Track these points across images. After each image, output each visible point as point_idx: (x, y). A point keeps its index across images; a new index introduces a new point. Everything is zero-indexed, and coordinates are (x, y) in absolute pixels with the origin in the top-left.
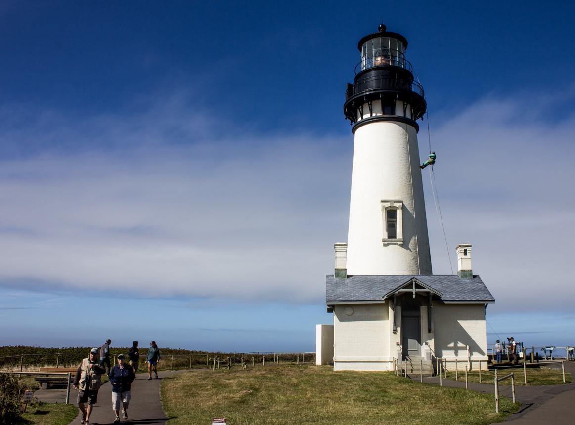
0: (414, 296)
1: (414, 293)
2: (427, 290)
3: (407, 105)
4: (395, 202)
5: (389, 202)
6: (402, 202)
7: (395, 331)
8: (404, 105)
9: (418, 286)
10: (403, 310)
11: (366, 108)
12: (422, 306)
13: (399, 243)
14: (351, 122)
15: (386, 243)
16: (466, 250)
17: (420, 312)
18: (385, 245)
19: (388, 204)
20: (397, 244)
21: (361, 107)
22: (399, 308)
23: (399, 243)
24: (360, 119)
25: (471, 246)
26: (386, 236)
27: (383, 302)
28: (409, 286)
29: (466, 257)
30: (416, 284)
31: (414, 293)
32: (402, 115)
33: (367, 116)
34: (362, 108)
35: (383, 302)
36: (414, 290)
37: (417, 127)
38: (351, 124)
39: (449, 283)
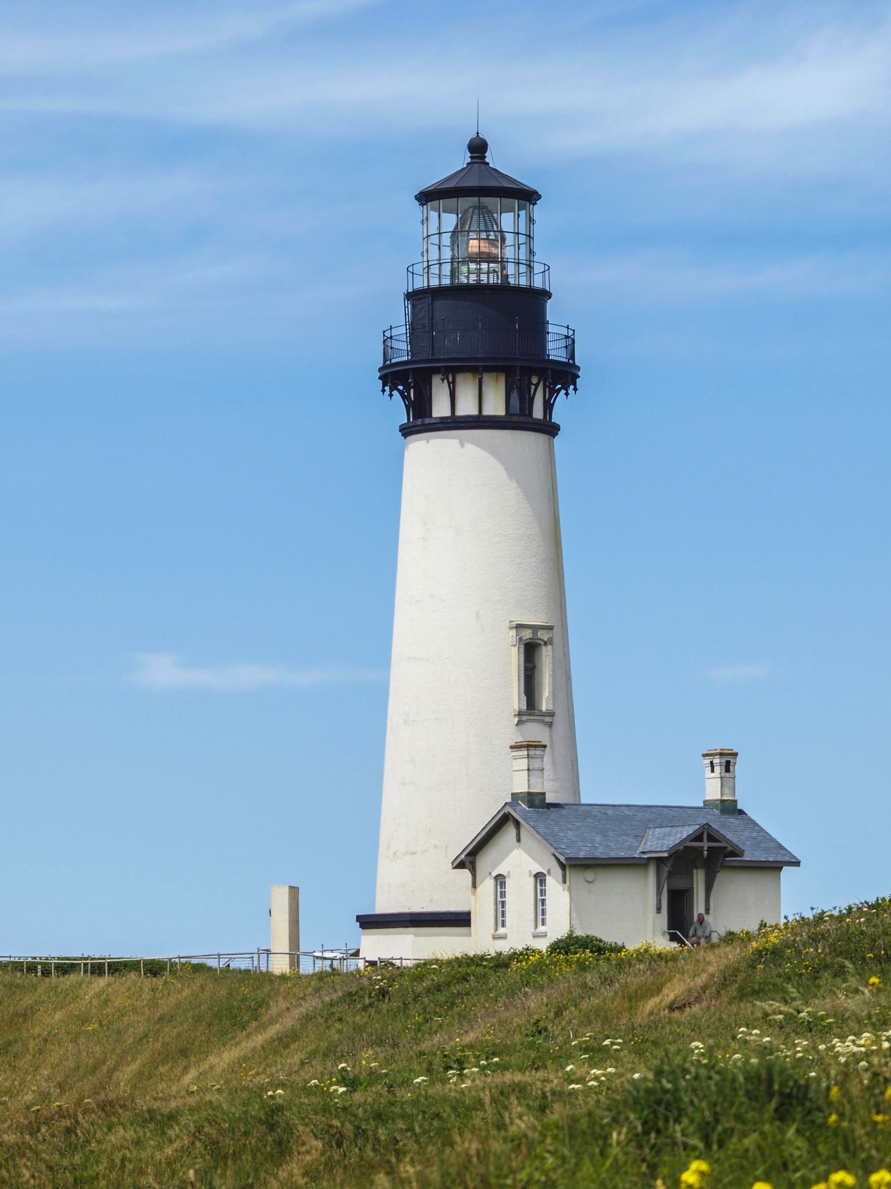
1: (706, 848)
7: (659, 910)
9: (711, 838)
12: (697, 868)
14: (384, 386)
15: (524, 718)
17: (692, 878)
20: (542, 721)
23: (548, 719)
24: (440, 408)
28: (698, 837)
29: (727, 775)
33: (467, 407)
34: (454, 382)
37: (550, 429)
38: (383, 391)
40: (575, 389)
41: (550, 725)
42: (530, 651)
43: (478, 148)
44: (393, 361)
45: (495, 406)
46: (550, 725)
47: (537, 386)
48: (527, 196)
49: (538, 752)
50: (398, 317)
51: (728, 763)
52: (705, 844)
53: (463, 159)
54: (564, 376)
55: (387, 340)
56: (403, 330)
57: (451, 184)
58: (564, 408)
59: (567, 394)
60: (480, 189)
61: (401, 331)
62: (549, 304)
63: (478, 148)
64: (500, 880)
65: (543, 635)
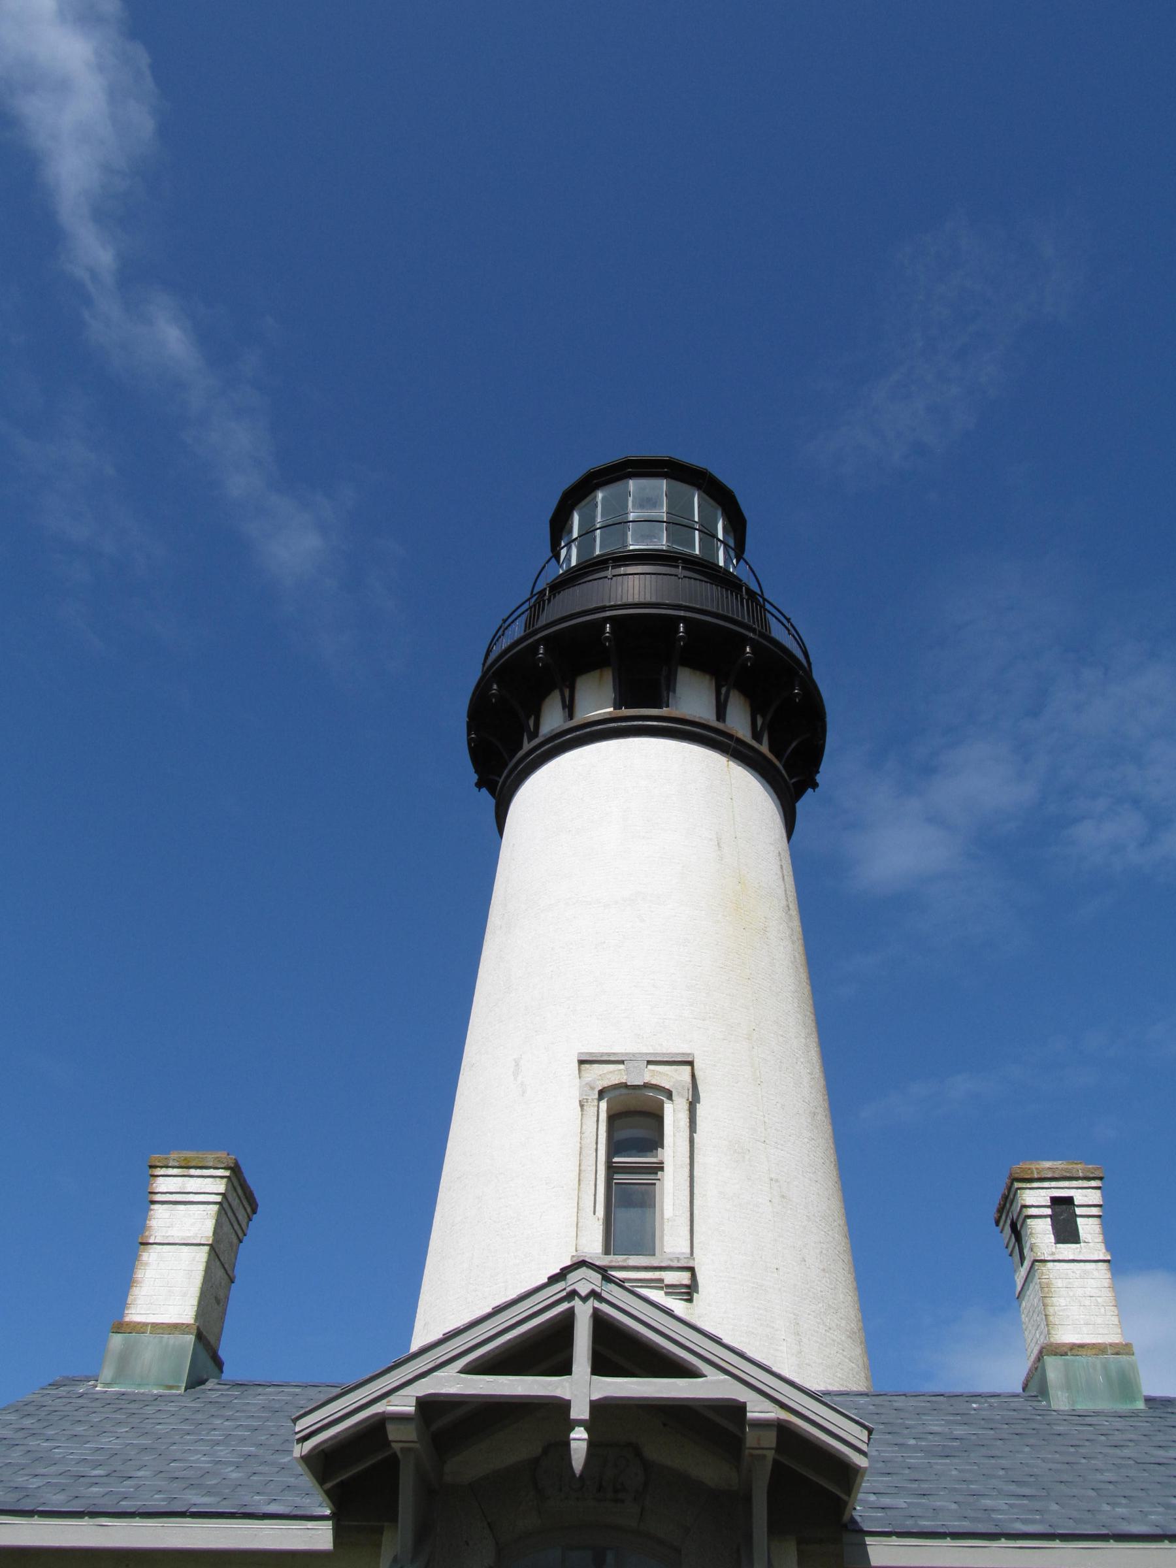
0: (579, 1434)
1: (580, 1411)
2: (710, 1387)
4: (649, 1062)
5: (622, 1062)
6: (691, 1063)
9: (620, 1349)
13: (671, 1277)
16: (1069, 1201)
23: (671, 1277)
29: (1067, 1250)
30: (600, 1323)
31: (580, 1411)
51: (1063, 1209)
52: (580, 1388)
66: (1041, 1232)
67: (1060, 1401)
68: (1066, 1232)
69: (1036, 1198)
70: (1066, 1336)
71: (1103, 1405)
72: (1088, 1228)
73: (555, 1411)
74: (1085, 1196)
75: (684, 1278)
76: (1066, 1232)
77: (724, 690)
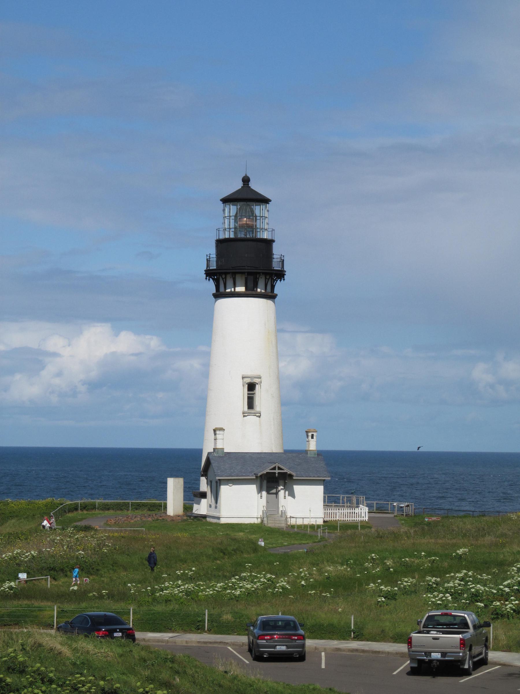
3: (268, 279)
8: (266, 278)
9: (279, 468)
10: (268, 482)
11: (230, 282)
13: (257, 415)
15: (246, 414)
18: (244, 416)
19: (248, 380)
20: (255, 415)
21: (224, 276)
22: (265, 483)
23: (257, 415)
24: (222, 289)
25: (316, 432)
26: (246, 408)
27: (254, 477)
28: (274, 468)
29: (312, 440)
32: (263, 291)
34: (226, 278)
35: (254, 477)
36: (277, 471)
38: (209, 280)
39: (300, 461)
40: (284, 280)
41: (259, 417)
42: (251, 387)
43: (246, 180)
44: (211, 268)
45: (241, 289)
46: (259, 417)
47: (258, 279)
48: (266, 201)
49: (221, 432)
50: (212, 251)
52: (277, 471)
53: (239, 185)
54: (280, 275)
55: (208, 261)
56: (215, 256)
57: (235, 197)
58: (279, 287)
59: (280, 281)
60: (246, 198)
61: (214, 256)
62: (274, 245)
63: (246, 180)
64: (211, 482)
65: (256, 380)
66: (310, 437)
67: (309, 456)
68: (312, 437)
69: (310, 434)
70: (311, 449)
71: (313, 456)
72: (315, 437)
73: (275, 473)
74: (315, 434)
75: (259, 415)
76: (312, 437)
77: (267, 280)
